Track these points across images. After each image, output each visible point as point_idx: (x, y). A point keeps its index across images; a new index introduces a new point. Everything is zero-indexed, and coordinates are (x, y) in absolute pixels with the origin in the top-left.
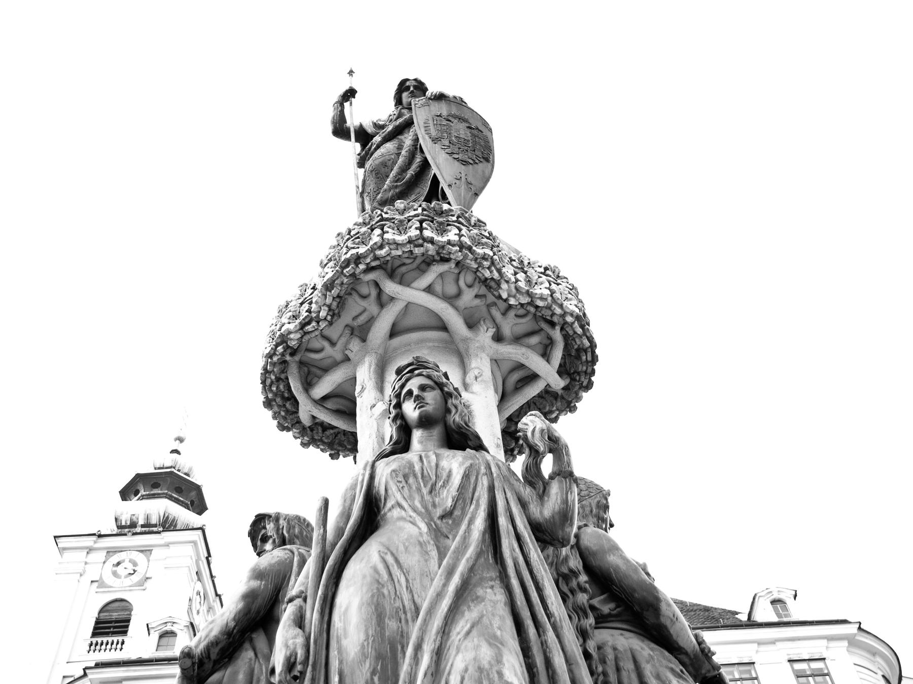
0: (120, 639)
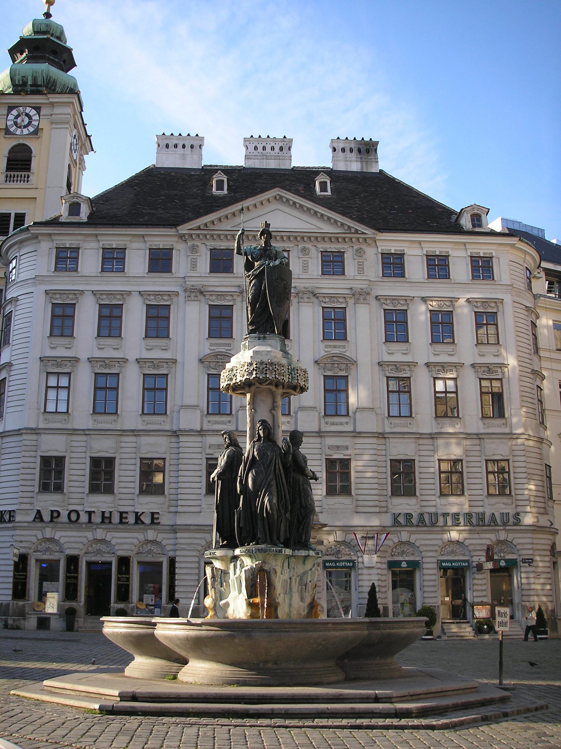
0: (26, 173)
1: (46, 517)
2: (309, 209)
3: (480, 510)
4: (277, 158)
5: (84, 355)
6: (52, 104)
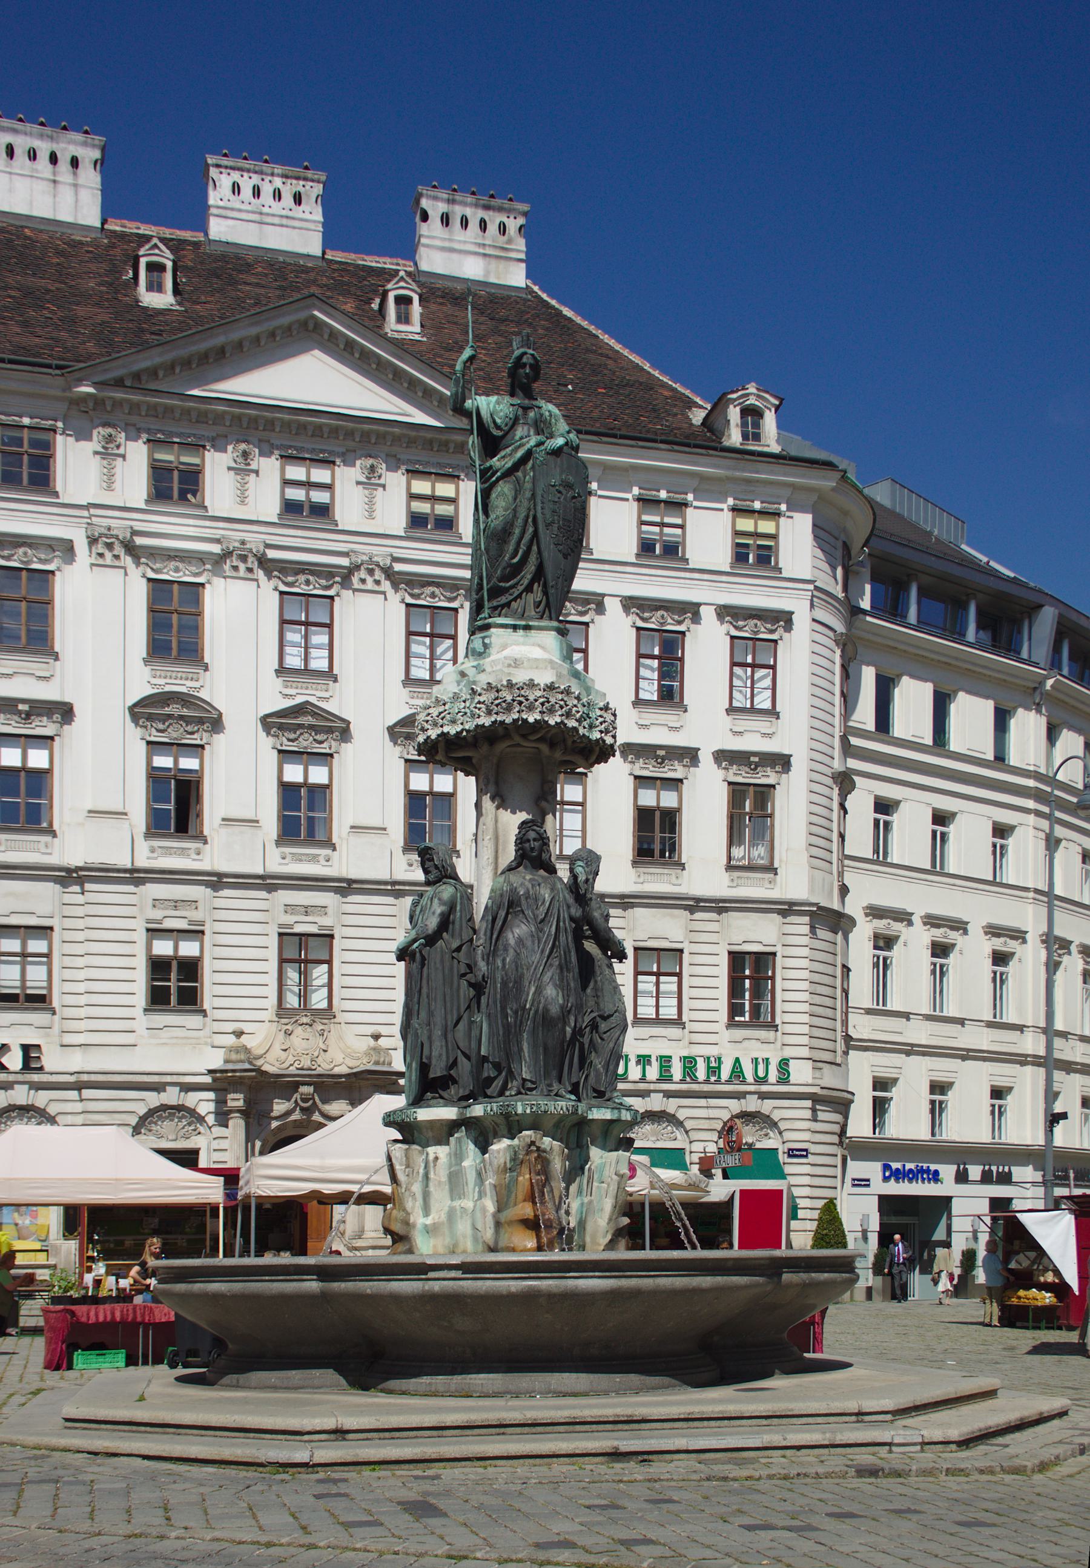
3: (712, 1051)
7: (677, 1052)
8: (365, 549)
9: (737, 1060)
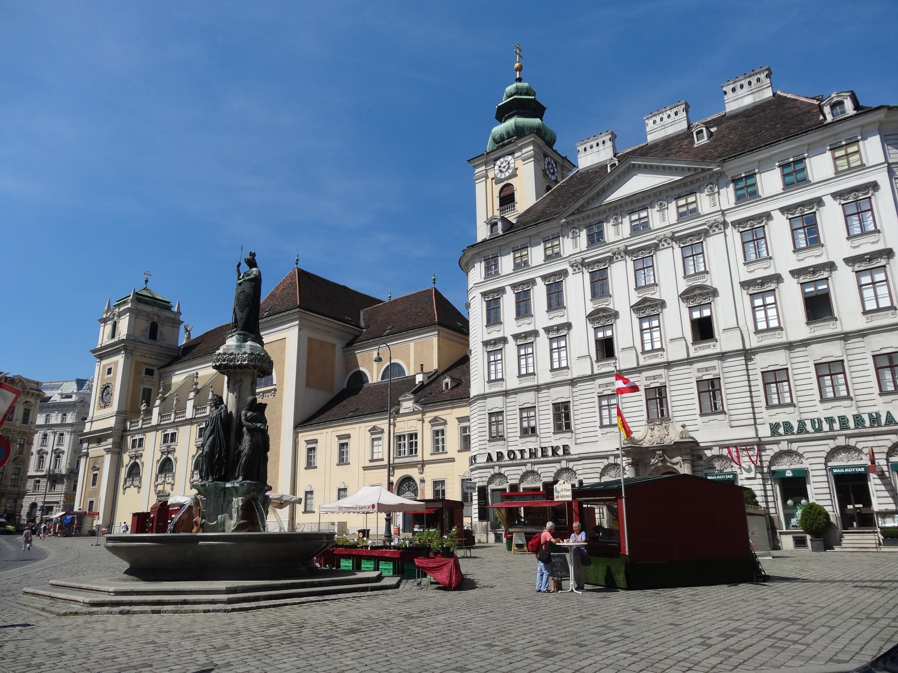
1: (495, 458)
2: (657, 167)
4: (673, 123)
5: (508, 335)
6: (520, 149)
7: (849, 413)
8: (661, 234)
9: (888, 412)
